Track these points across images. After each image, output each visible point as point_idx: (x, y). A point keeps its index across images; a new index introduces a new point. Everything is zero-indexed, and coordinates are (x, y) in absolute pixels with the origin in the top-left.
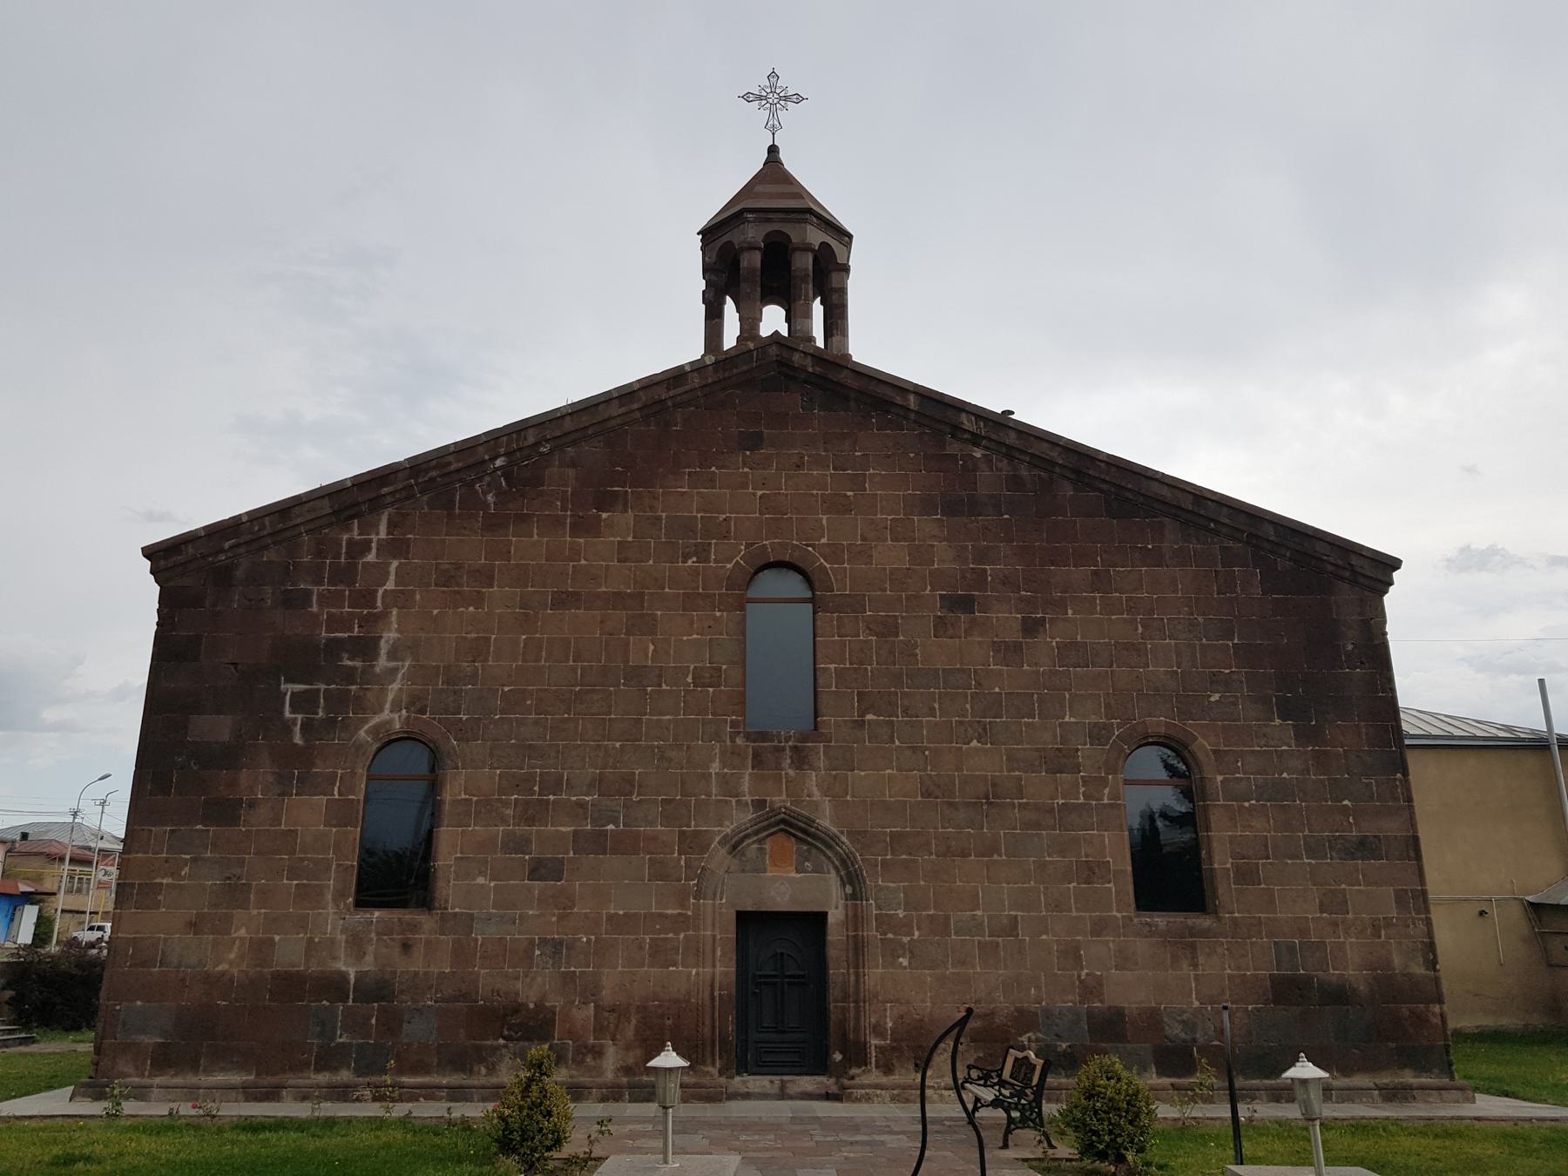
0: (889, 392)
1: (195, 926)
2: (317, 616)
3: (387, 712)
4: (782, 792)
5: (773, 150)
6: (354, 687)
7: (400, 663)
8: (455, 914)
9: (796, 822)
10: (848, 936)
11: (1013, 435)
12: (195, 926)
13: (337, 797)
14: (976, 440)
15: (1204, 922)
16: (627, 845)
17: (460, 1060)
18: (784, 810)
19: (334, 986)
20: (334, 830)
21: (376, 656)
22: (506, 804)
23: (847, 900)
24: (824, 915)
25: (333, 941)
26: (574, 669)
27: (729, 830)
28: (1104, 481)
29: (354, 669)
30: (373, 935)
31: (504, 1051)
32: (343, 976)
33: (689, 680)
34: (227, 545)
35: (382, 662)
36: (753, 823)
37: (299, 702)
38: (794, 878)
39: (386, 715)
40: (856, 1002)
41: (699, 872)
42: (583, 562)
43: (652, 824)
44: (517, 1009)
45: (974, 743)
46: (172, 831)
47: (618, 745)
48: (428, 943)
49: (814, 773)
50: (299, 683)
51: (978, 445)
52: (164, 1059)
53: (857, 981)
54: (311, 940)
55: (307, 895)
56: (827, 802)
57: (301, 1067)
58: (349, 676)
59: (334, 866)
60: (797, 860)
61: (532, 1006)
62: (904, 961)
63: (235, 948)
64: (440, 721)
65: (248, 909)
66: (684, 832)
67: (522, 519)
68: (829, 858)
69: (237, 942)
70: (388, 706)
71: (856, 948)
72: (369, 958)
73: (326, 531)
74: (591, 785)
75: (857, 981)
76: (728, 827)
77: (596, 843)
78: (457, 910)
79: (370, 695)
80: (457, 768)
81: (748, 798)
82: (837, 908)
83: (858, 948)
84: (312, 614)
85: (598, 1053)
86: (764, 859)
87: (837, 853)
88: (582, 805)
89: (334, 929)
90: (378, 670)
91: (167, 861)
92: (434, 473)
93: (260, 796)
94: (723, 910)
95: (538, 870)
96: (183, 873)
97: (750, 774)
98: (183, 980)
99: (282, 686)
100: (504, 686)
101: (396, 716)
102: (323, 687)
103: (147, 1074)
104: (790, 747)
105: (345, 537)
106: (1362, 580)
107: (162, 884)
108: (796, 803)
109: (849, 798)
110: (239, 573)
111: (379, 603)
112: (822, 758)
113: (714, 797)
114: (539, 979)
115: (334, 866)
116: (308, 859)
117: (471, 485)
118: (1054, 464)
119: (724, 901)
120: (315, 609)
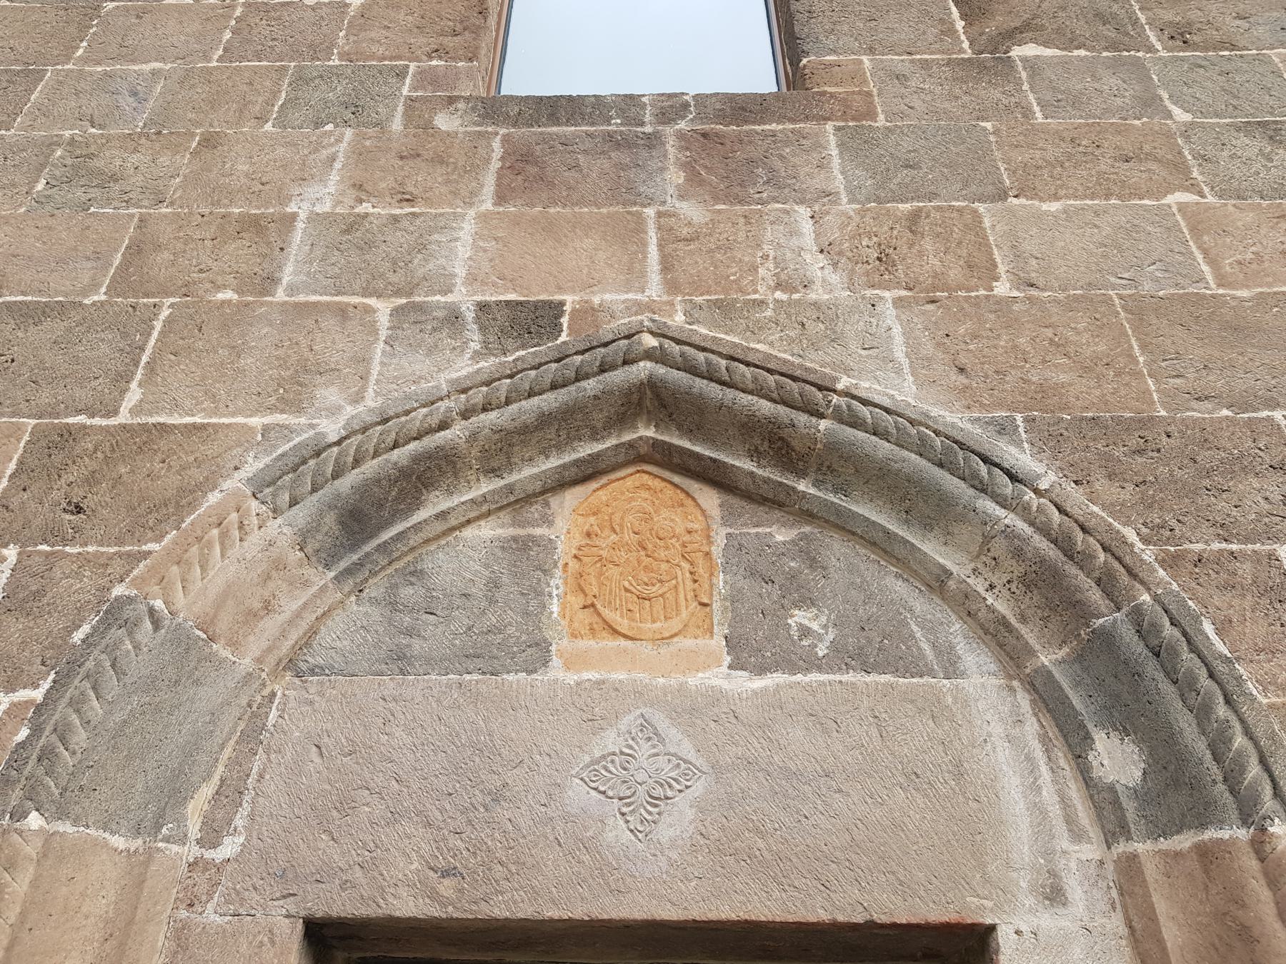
4: (643, 274)
9: (714, 391)
18: (650, 341)
23: (1115, 829)
36: (478, 395)
38: (715, 697)
41: (78, 636)
49: (803, 212)
56: (889, 311)
60: (734, 598)
66: (69, 435)
68: (937, 582)
76: (334, 411)
82: (1054, 895)
86: (539, 593)
87: (988, 535)
94: (212, 915)
97: (484, 218)
104: (680, 136)
109: (1002, 288)
112: (836, 162)
113: (280, 295)
119: (229, 848)
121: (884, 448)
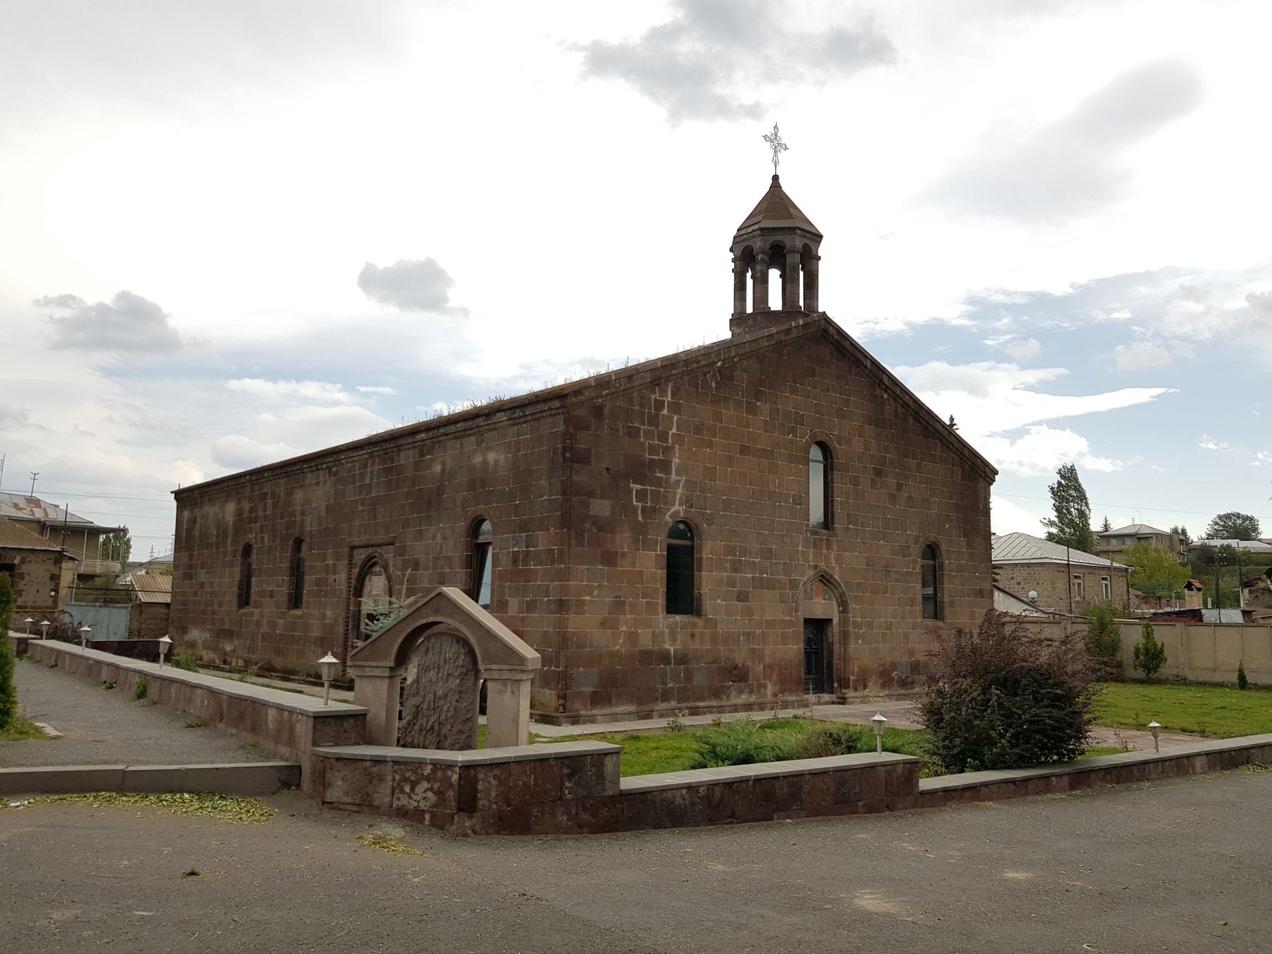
0: (860, 356)
1: (603, 624)
2: (643, 444)
3: (677, 505)
5: (775, 178)
6: (662, 490)
7: (680, 478)
8: (710, 618)
10: (840, 630)
11: (899, 390)
12: (603, 624)
13: (659, 552)
14: (886, 389)
15: (940, 624)
16: (770, 585)
17: (717, 693)
19: (664, 657)
20: (659, 571)
21: (670, 474)
22: (727, 561)
24: (832, 620)
25: (663, 632)
26: (749, 489)
27: (805, 579)
28: (924, 419)
29: (661, 478)
30: (679, 630)
31: (732, 687)
32: (669, 651)
33: (791, 500)
34: (605, 393)
35: (674, 477)
37: (641, 495)
39: (676, 507)
40: (844, 660)
42: (751, 429)
43: (779, 574)
44: (736, 667)
45: (882, 542)
46: (588, 569)
47: (766, 532)
48: (701, 633)
50: (638, 484)
51: (886, 392)
52: (600, 698)
53: (845, 650)
54: (654, 632)
55: (651, 608)
57: (655, 700)
58: (659, 482)
59: (661, 592)
61: (741, 665)
62: (860, 641)
63: (622, 637)
64: (699, 513)
65: (625, 614)
67: (727, 399)
68: (834, 594)
69: (623, 633)
70: (677, 502)
71: (844, 636)
72: (678, 642)
73: (644, 391)
74: (757, 554)
75: (845, 650)
77: (759, 583)
78: (711, 616)
79: (670, 496)
80: (707, 540)
81: (811, 564)
83: (845, 635)
84: (640, 442)
85: (765, 687)
88: (754, 563)
89: (663, 626)
90: (672, 480)
91: (587, 586)
92: (694, 366)
93: (626, 550)
95: (742, 597)
96: (595, 594)
98: (600, 656)
99: (631, 485)
100: (723, 496)
101: (681, 508)
102: (649, 488)
103: (589, 708)
105: (653, 397)
106: (987, 478)
107: (585, 600)
108: (827, 567)
110: (606, 411)
111: (670, 441)
114: (743, 652)
115: (661, 592)
116: (651, 588)
117: (705, 374)
118: (909, 406)
120: (642, 440)
121: (835, 583)
